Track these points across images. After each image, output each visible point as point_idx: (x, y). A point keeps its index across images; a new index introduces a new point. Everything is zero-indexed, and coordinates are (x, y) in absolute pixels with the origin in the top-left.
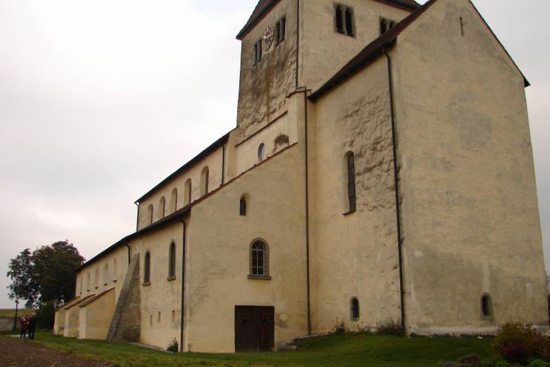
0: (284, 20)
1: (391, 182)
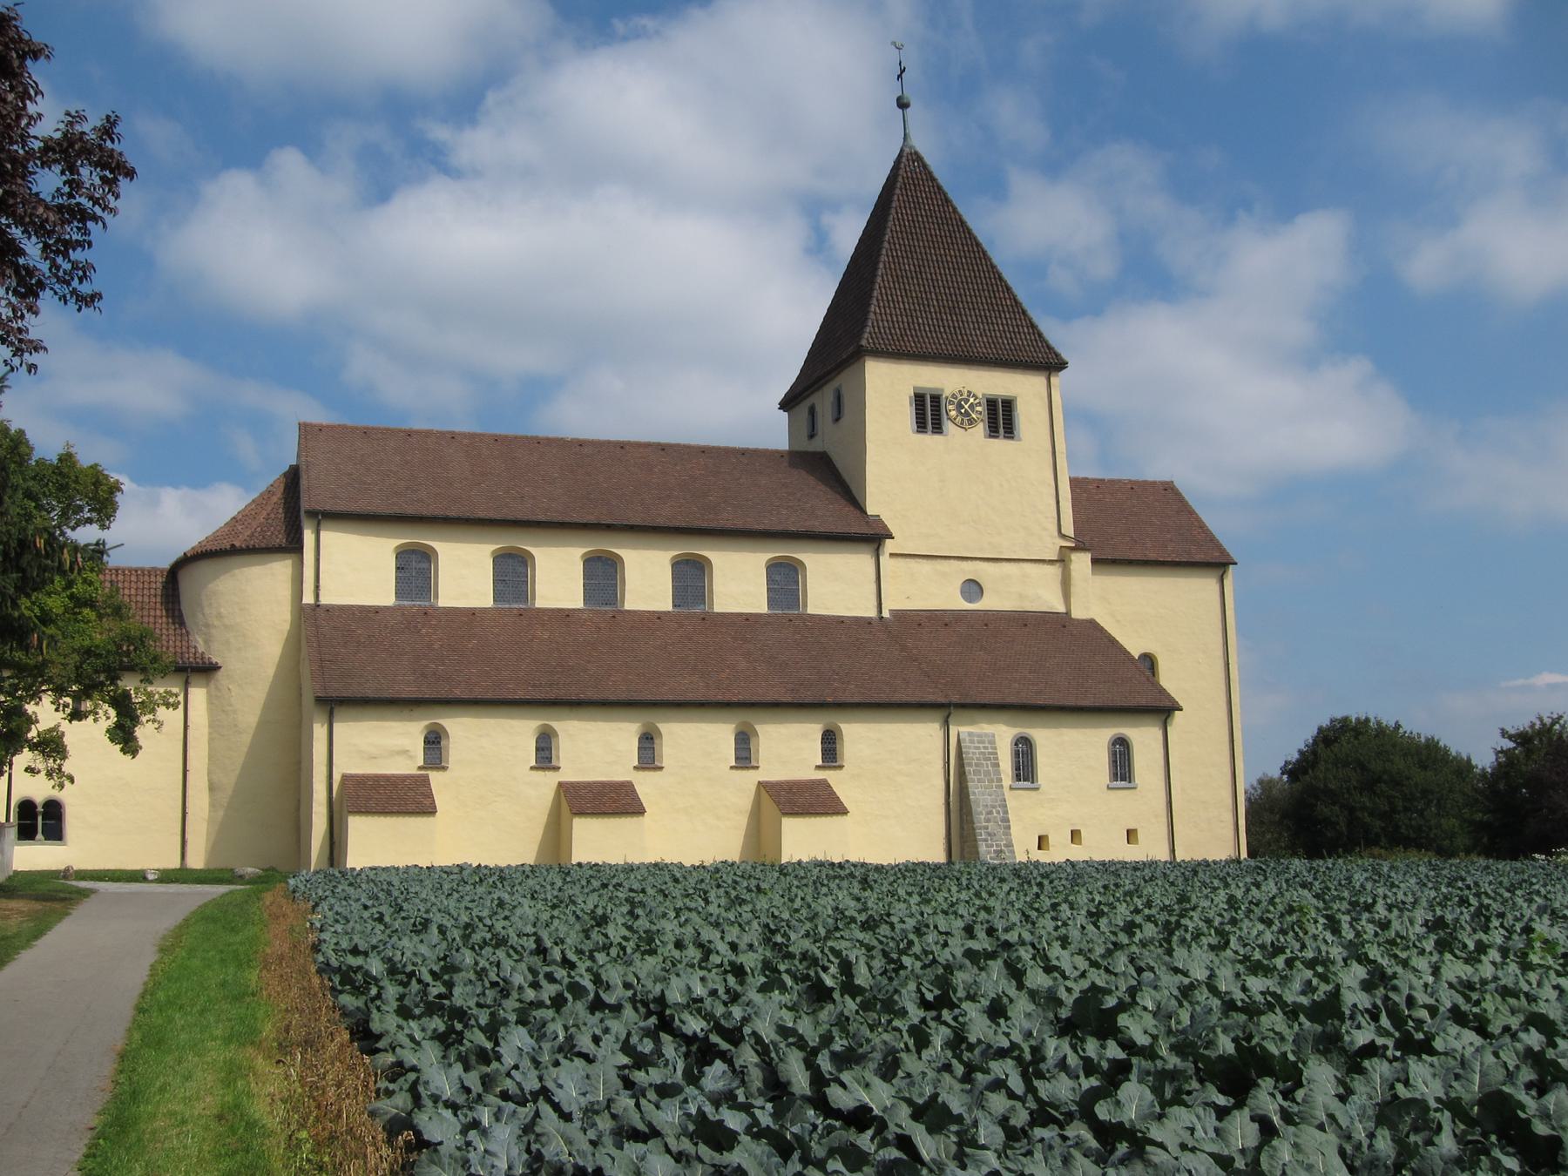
0: (1009, 405)
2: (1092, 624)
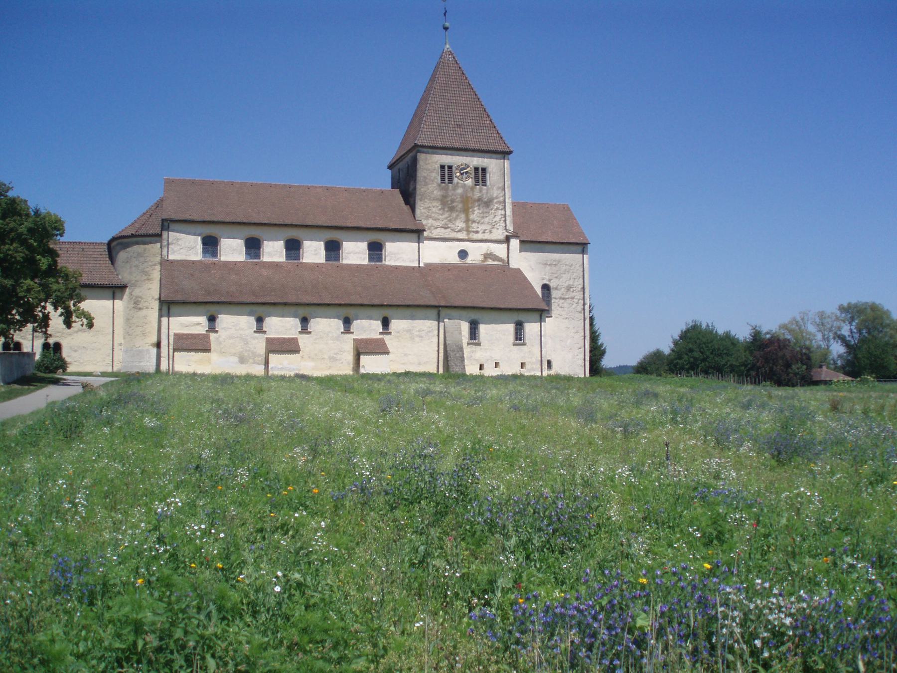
0: (484, 170)
1: (580, 307)
2: (518, 271)
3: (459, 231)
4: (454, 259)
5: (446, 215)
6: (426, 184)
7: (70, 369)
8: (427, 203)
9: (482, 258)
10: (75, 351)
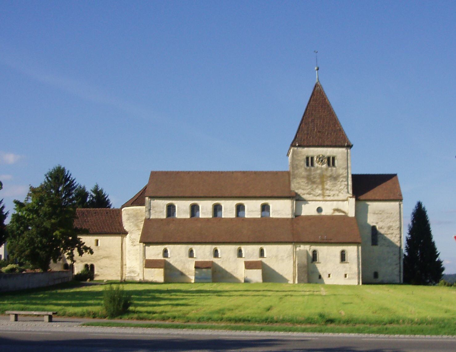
0: (334, 159)
3: (318, 196)
4: (314, 213)
5: (309, 187)
6: (298, 169)
7: (96, 279)
8: (299, 180)
9: (332, 211)
10: (102, 269)
